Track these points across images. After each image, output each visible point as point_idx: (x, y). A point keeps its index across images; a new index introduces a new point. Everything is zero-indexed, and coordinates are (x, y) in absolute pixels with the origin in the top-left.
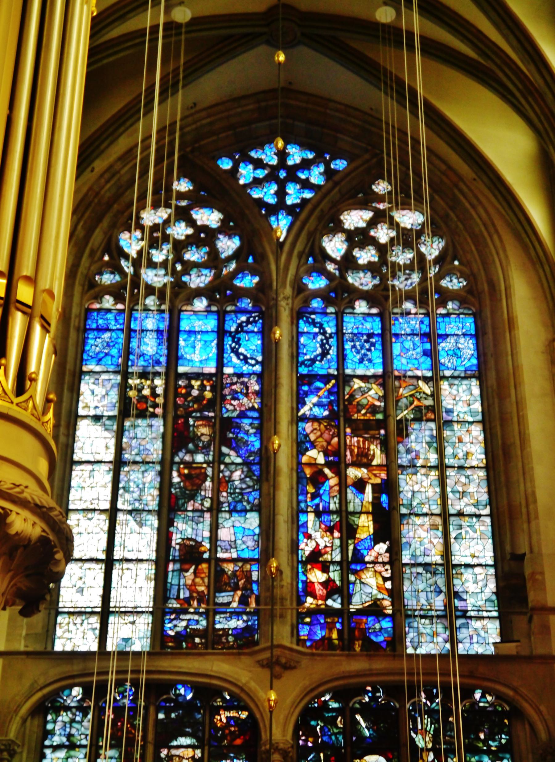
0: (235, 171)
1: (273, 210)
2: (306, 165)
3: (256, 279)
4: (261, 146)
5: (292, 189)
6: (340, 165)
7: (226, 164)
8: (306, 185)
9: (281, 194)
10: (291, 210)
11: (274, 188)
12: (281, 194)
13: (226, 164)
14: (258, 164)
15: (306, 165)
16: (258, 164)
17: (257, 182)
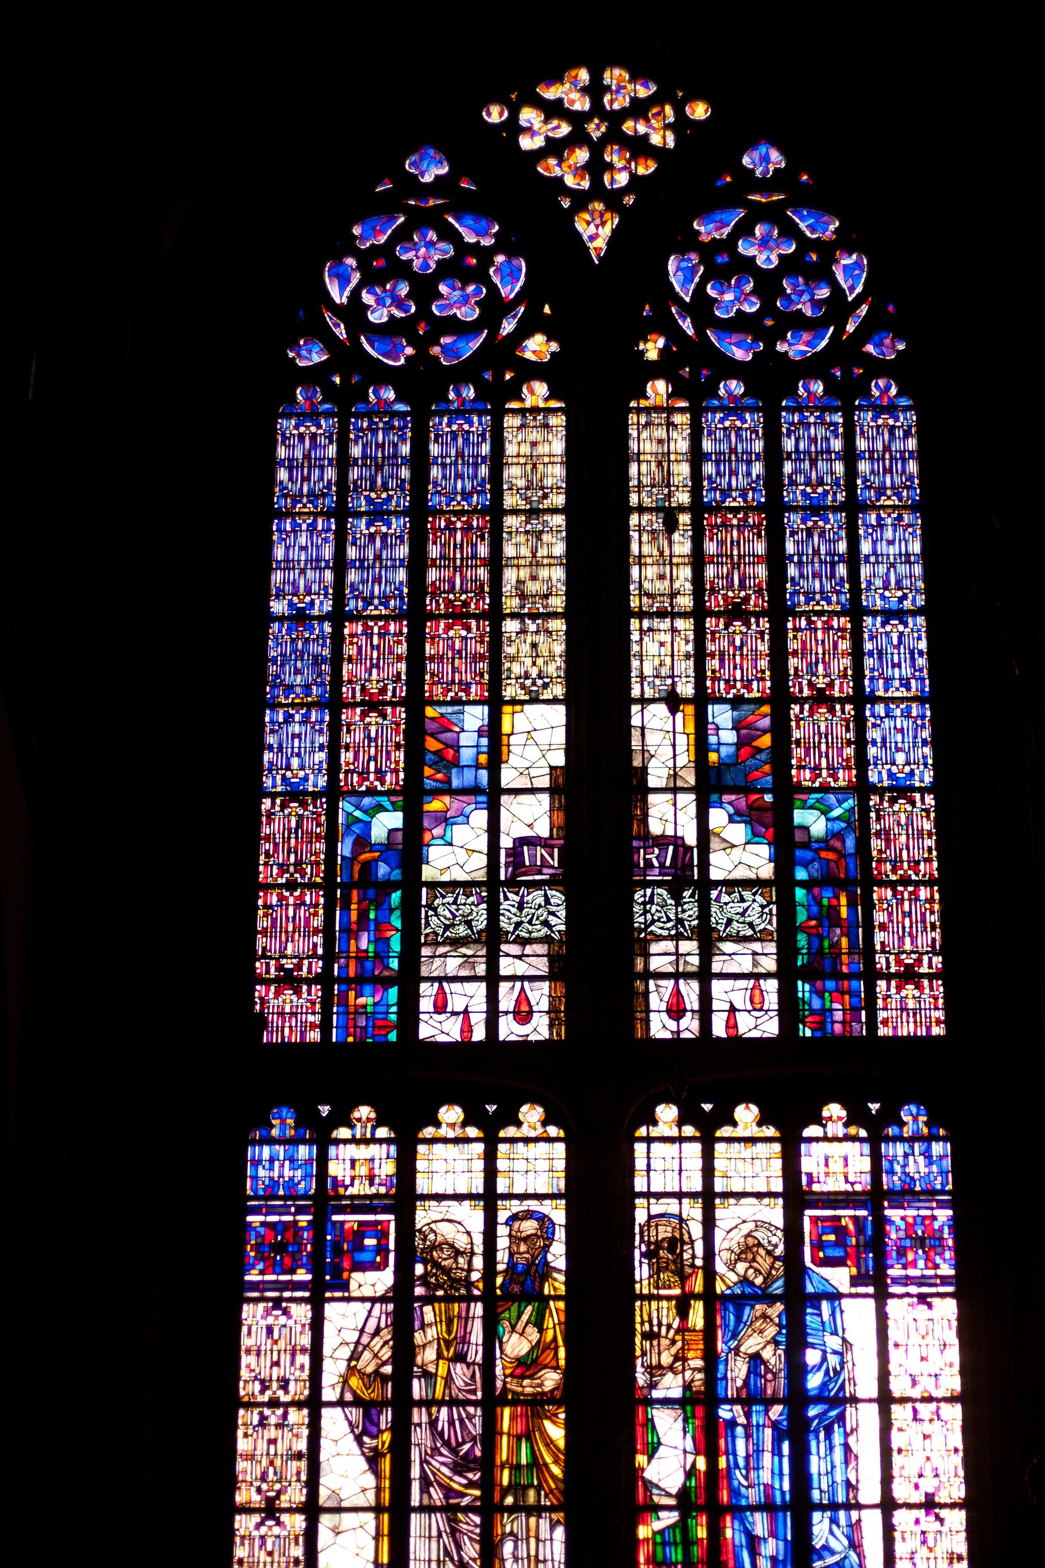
0: (513, 128)
1: (581, 200)
2: (638, 109)
3: (554, 347)
4: (557, 78)
5: (614, 156)
6: (699, 111)
7: (495, 115)
8: (639, 147)
9: (596, 167)
10: (612, 199)
11: (581, 156)
12: (596, 167)
13: (495, 115)
14: (554, 110)
15: (638, 109)
16: (554, 110)
17: (555, 148)
